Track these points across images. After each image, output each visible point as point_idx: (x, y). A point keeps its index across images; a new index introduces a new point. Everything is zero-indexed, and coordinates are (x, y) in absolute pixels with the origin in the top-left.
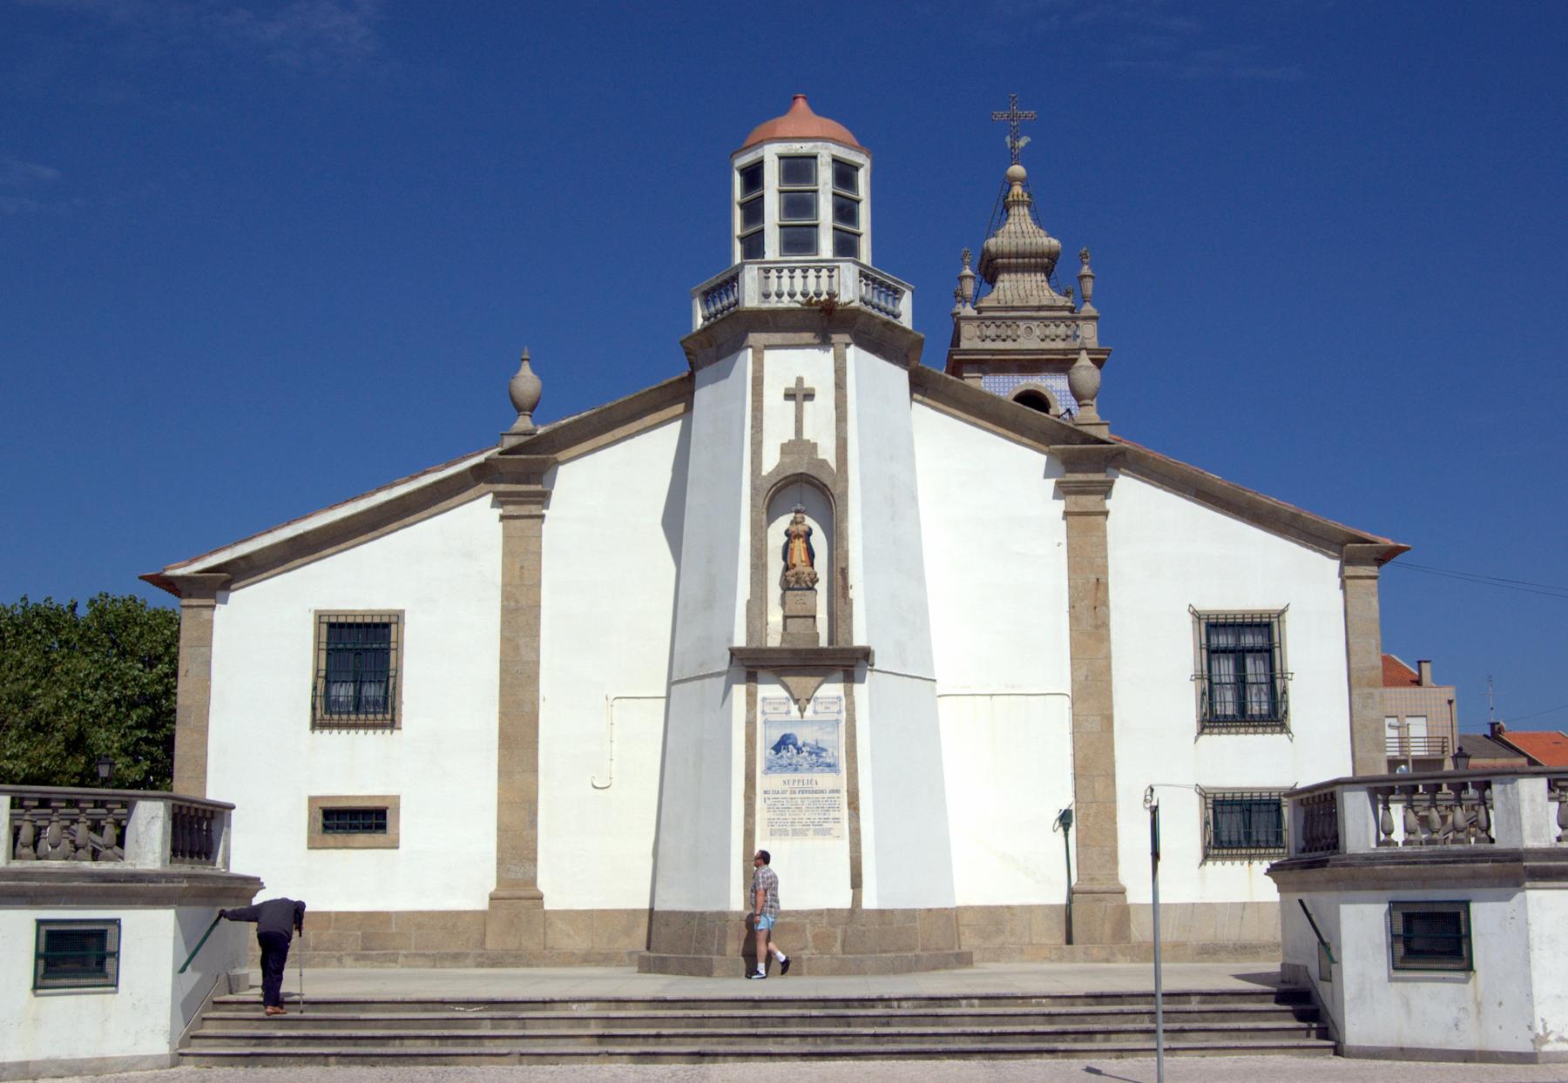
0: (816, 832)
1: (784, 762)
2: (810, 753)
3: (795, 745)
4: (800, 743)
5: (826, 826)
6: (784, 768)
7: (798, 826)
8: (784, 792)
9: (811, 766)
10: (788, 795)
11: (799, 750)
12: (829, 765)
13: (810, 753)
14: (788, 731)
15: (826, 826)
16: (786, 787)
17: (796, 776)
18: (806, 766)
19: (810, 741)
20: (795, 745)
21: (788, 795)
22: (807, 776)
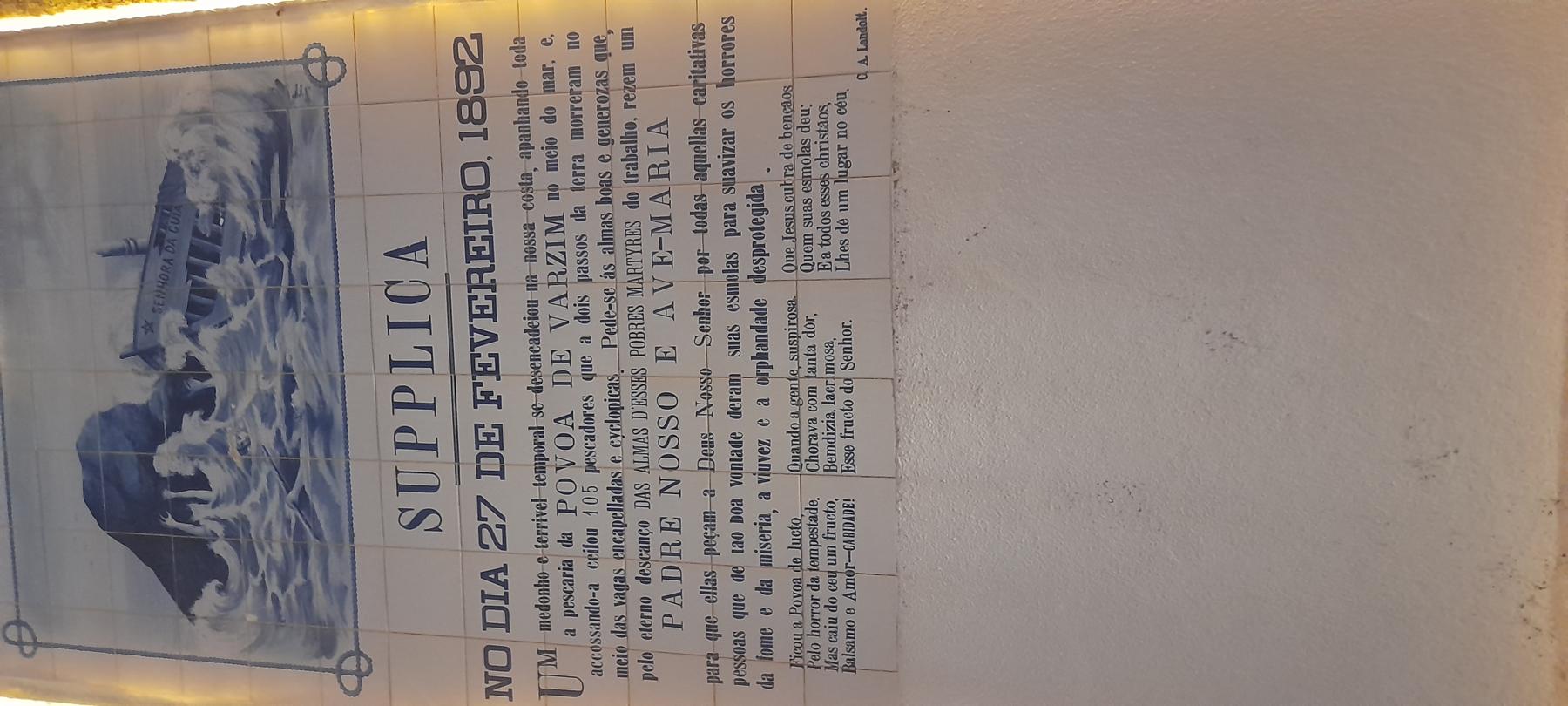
0: (821, 254)
1: (269, 515)
2: (202, 306)
3: (151, 427)
4: (139, 388)
5: (760, 158)
6: (317, 522)
7: (771, 418)
8: (492, 532)
9: (291, 297)
10: (514, 495)
11: (186, 395)
12: (275, 147)
13: (202, 306)
14: (69, 479)
15: (760, 158)
16: (454, 505)
17: (367, 417)
18: (293, 329)
19: (113, 306)
20: (151, 427)
21: (514, 495)
22: (367, 346)
